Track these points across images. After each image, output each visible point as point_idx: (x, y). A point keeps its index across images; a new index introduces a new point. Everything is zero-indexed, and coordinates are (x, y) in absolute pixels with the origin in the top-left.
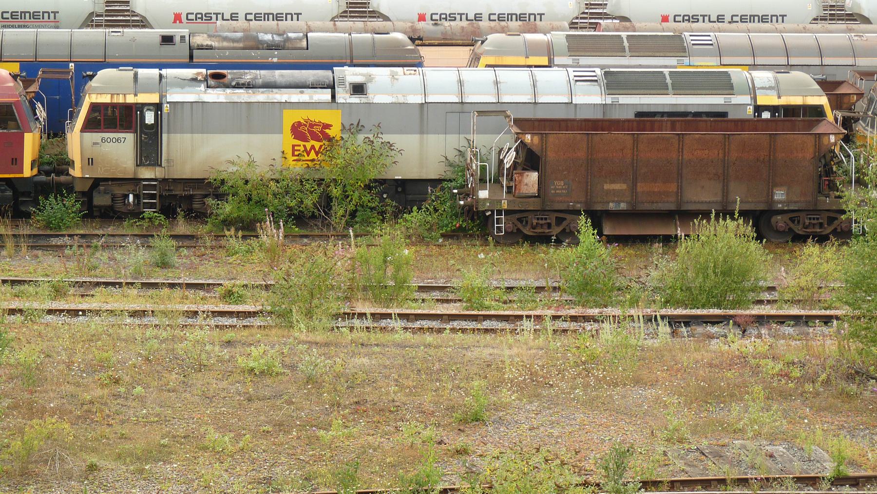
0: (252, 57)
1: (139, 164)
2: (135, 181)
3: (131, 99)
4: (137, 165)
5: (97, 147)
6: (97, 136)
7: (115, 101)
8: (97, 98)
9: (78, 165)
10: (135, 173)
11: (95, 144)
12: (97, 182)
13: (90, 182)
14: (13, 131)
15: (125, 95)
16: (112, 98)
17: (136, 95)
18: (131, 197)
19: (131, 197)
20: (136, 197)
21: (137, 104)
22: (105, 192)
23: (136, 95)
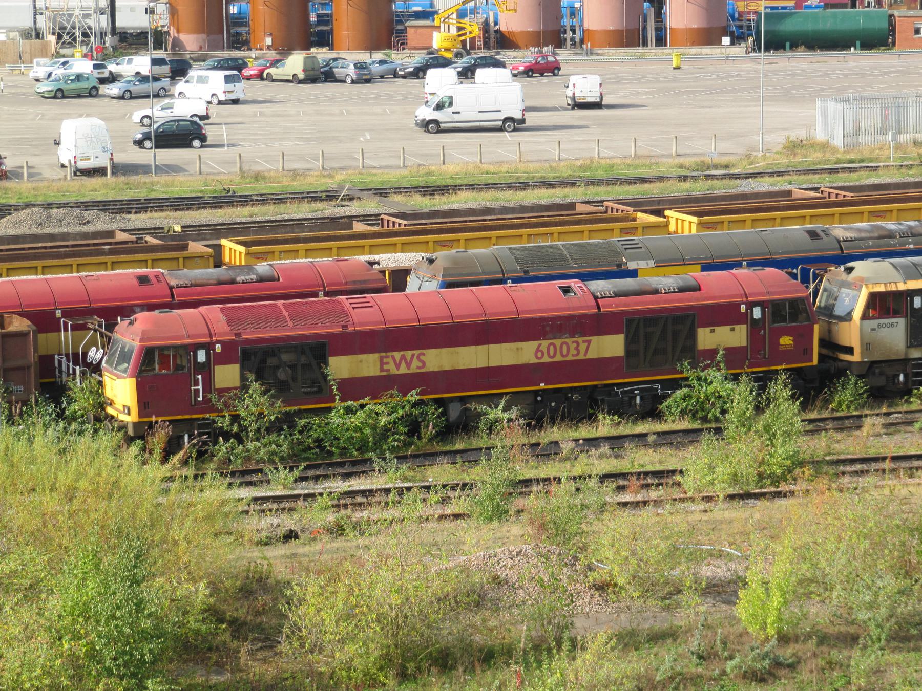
0: (891, 245)
1: (910, 346)
2: (906, 361)
3: (902, 287)
4: (908, 347)
5: (874, 334)
6: (874, 323)
7: (889, 289)
8: (873, 288)
9: (857, 350)
10: (906, 354)
11: (873, 330)
12: (873, 364)
13: (867, 365)
14: (805, 323)
15: (896, 283)
16: (886, 287)
17: (905, 283)
18: (901, 378)
19: (901, 378)
20: (906, 376)
21: (908, 290)
22: (881, 374)
23: (905, 283)
